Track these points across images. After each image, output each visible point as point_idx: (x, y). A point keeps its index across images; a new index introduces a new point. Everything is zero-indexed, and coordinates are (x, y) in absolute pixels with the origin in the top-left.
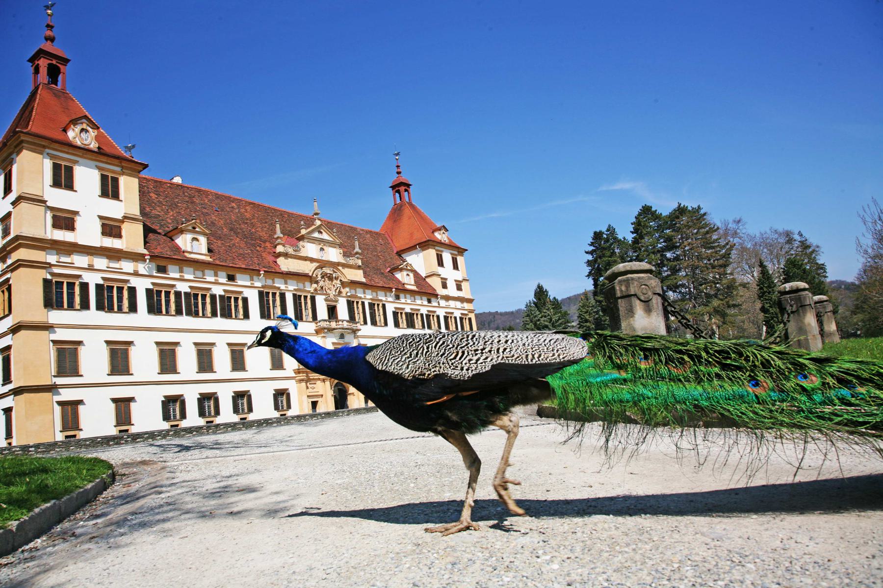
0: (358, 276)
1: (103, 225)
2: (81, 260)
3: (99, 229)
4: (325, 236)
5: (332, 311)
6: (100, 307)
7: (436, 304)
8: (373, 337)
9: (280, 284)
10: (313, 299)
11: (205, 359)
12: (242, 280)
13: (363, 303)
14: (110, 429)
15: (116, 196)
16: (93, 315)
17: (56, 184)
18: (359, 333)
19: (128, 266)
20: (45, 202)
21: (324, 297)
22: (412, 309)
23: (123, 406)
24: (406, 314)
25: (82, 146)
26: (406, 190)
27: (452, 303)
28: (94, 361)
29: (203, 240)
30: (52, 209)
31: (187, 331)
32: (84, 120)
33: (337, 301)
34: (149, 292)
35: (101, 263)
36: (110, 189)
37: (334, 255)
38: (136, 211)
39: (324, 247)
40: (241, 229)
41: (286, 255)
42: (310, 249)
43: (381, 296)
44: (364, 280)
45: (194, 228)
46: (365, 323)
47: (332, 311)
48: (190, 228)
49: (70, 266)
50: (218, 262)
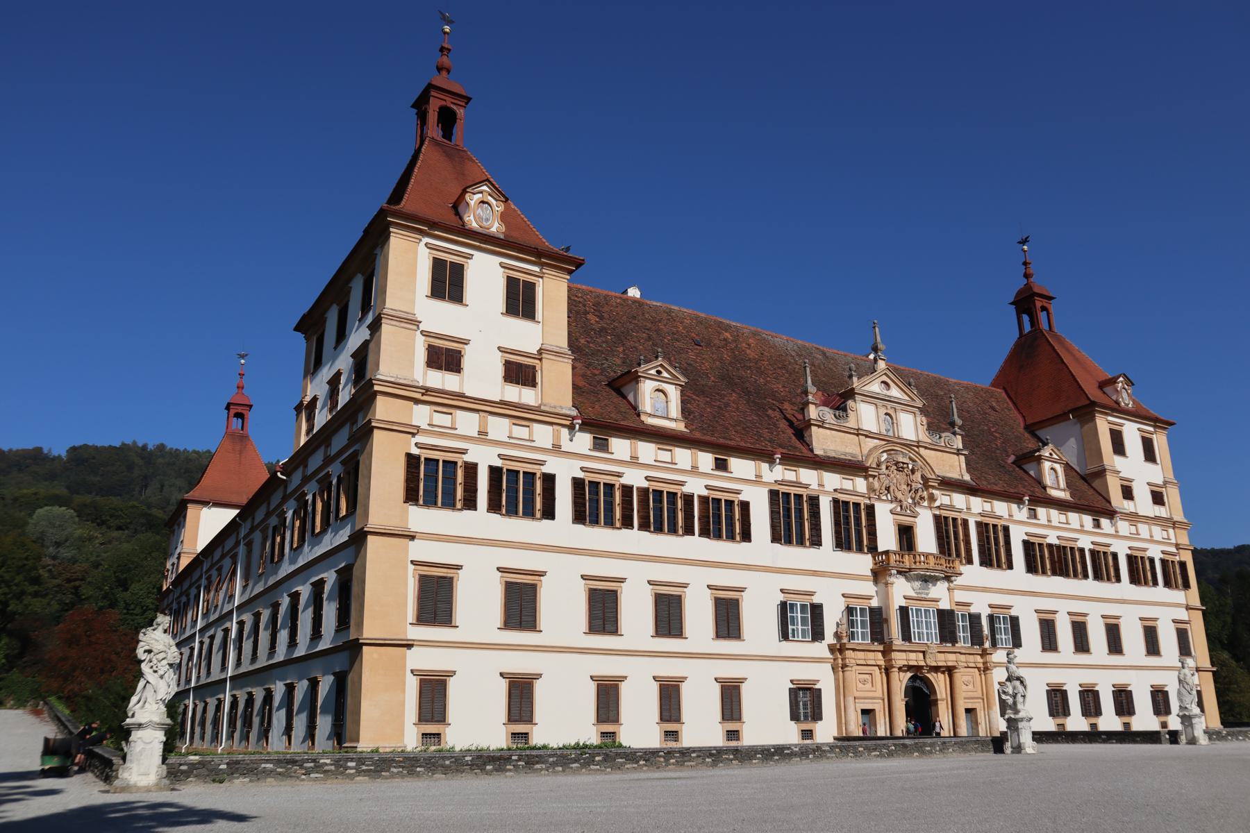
0: (955, 467)
1: (508, 364)
2: (467, 423)
3: (500, 370)
4: (895, 392)
5: (906, 534)
6: (494, 506)
8: (985, 590)
9: (808, 476)
10: (871, 510)
11: (668, 614)
12: (740, 467)
13: (965, 522)
14: (496, 737)
15: (529, 314)
16: (481, 521)
17: (437, 291)
18: (959, 581)
19: (543, 435)
20: (417, 323)
21: (893, 506)
23: (521, 692)
24: (1050, 546)
25: (480, 230)
26: (1044, 309)
27: (1144, 530)
28: (479, 602)
29: (674, 393)
30: (425, 334)
31: (641, 560)
32: (485, 188)
34: (578, 484)
35: (499, 428)
36: (520, 301)
37: (910, 426)
38: (561, 340)
40: (740, 378)
43: (1001, 508)
44: (967, 477)
45: (659, 372)
46: (970, 561)
47: (906, 534)
48: (653, 372)
49: (450, 431)
50: (698, 435)
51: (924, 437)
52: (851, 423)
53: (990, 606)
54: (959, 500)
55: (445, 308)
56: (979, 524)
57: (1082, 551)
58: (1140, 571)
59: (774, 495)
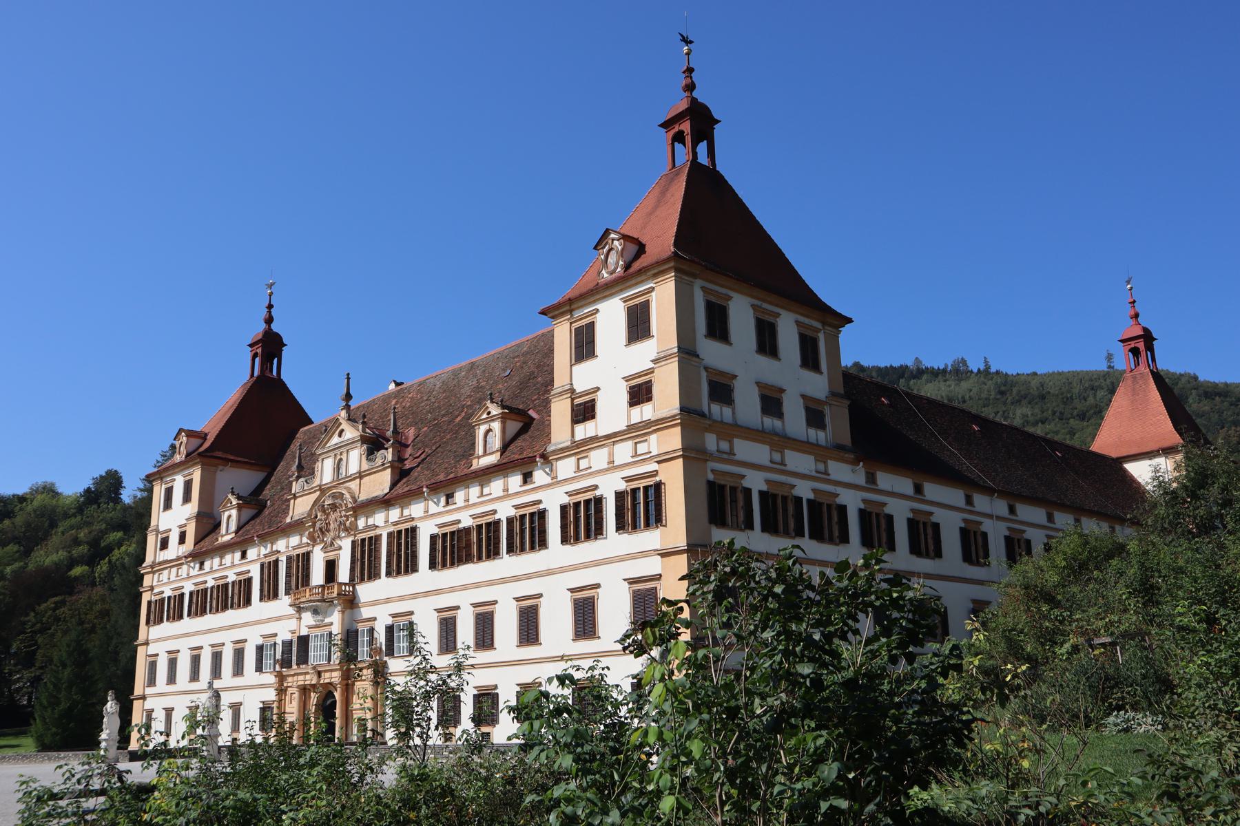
5: (331, 567)
7: (548, 480)
8: (387, 601)
9: (281, 545)
22: (473, 517)
33: (340, 548)
37: (355, 459)
39: (344, 457)
41: (295, 497)
42: (326, 471)
43: (416, 509)
47: (331, 567)
51: (365, 466)
52: (317, 482)
53: (394, 616)
54: (379, 518)
55: (168, 512)
56: (390, 535)
57: (497, 523)
58: (583, 521)
59: (262, 566)
